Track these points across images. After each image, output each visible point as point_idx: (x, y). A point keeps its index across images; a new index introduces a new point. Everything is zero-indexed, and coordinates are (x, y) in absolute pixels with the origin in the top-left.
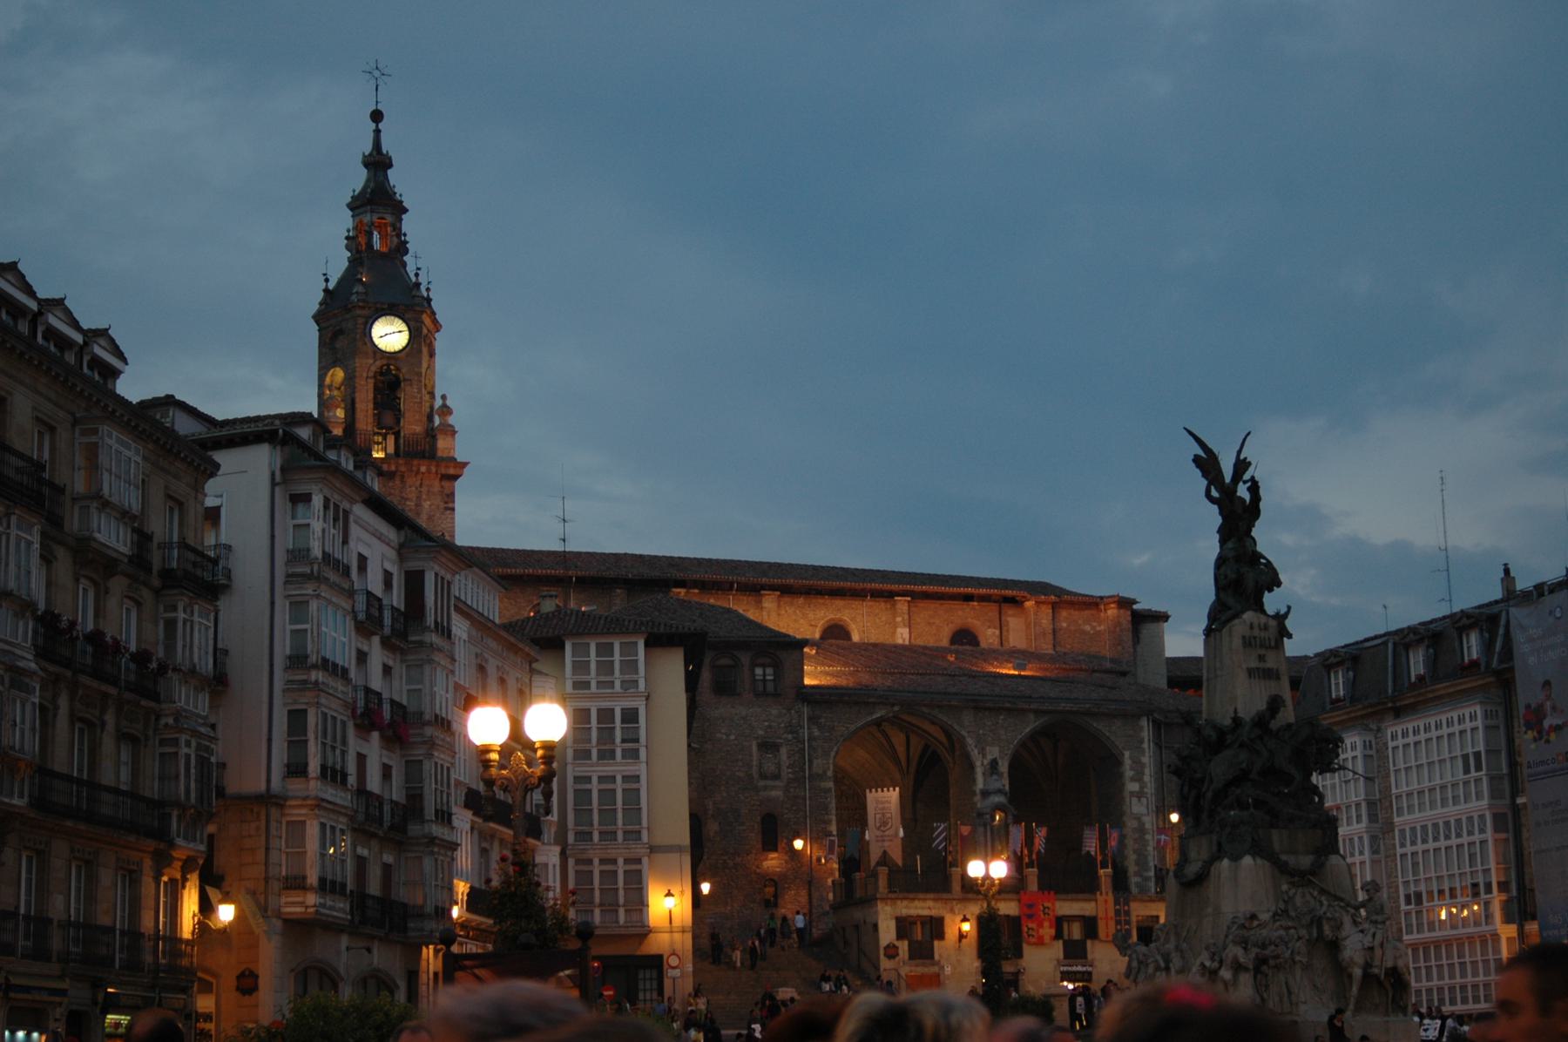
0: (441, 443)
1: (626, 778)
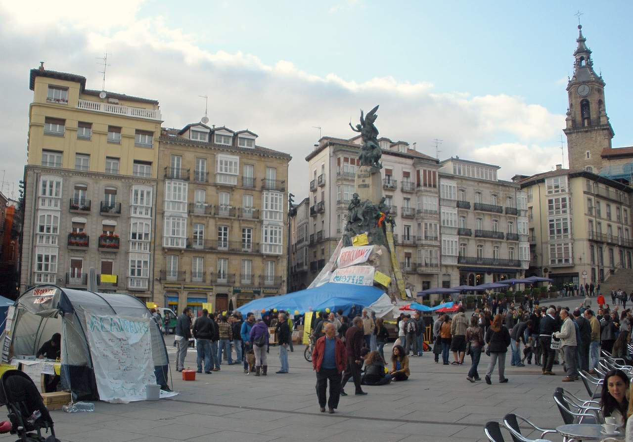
0: (602, 119)
1: (563, 219)
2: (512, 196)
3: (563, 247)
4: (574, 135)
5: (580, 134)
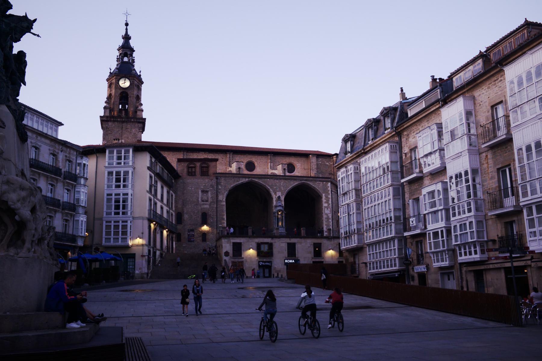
0: (138, 113)
2: (73, 159)
3: (121, 224)
4: (110, 124)
5: (116, 123)
